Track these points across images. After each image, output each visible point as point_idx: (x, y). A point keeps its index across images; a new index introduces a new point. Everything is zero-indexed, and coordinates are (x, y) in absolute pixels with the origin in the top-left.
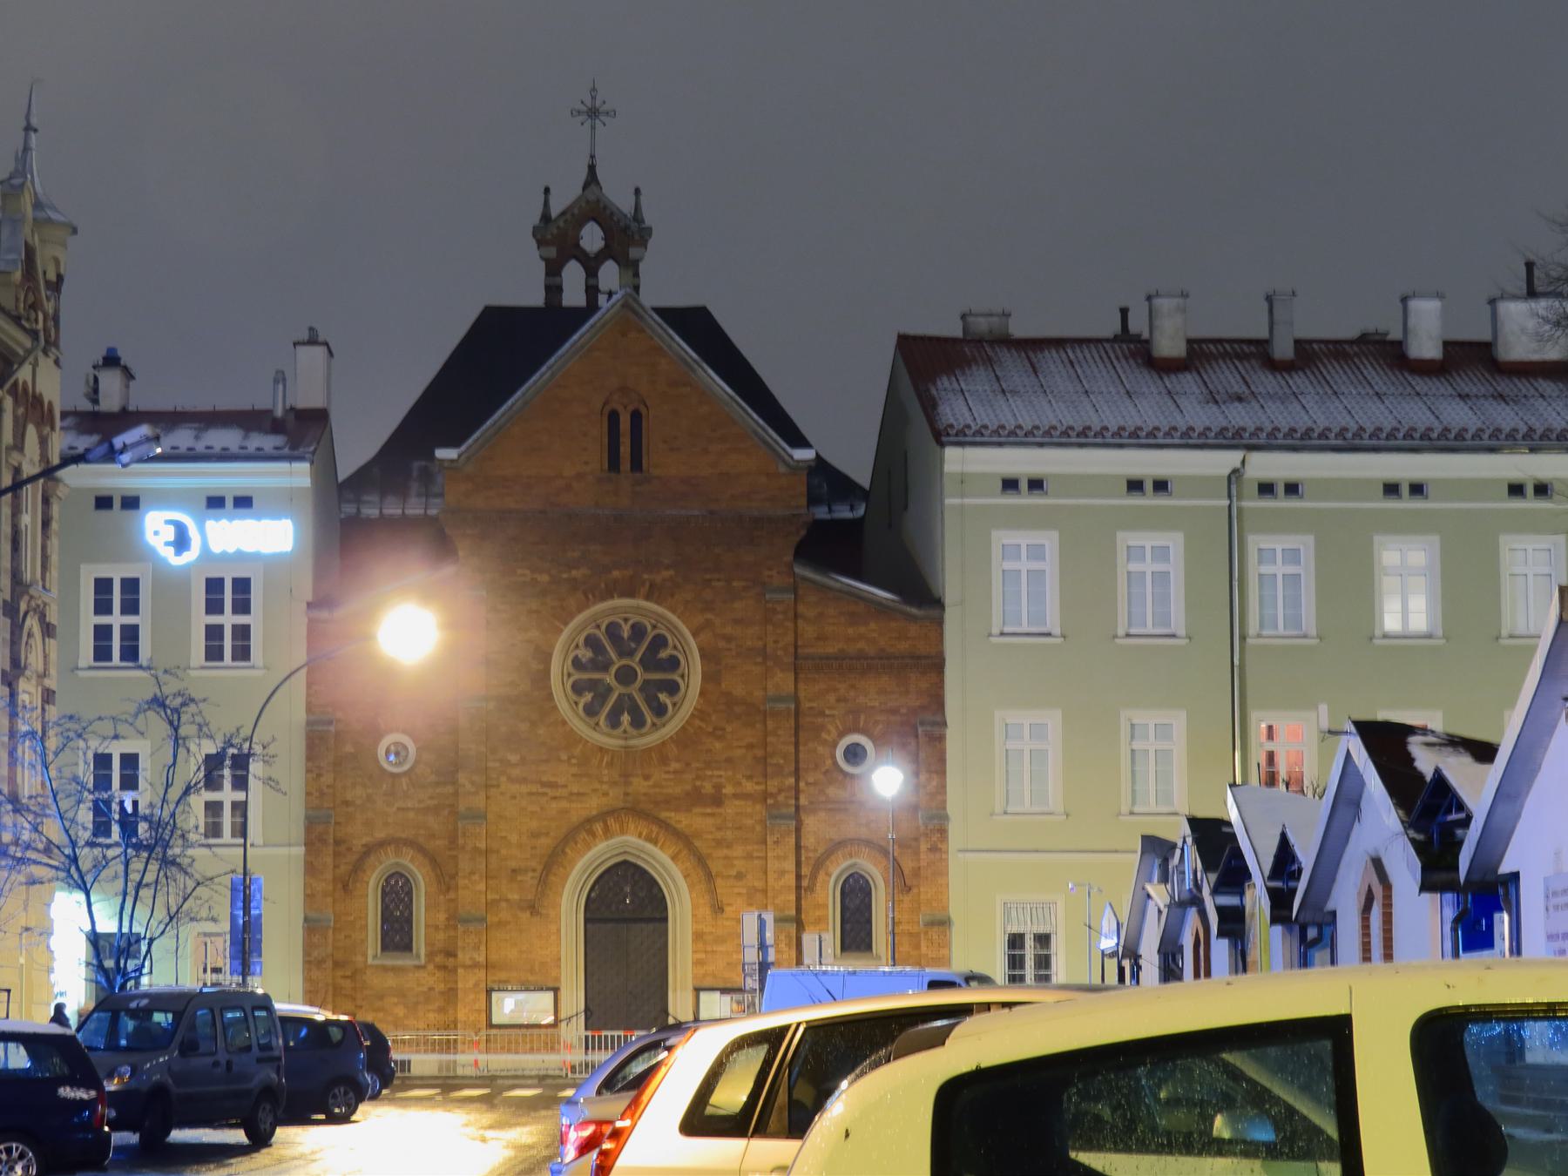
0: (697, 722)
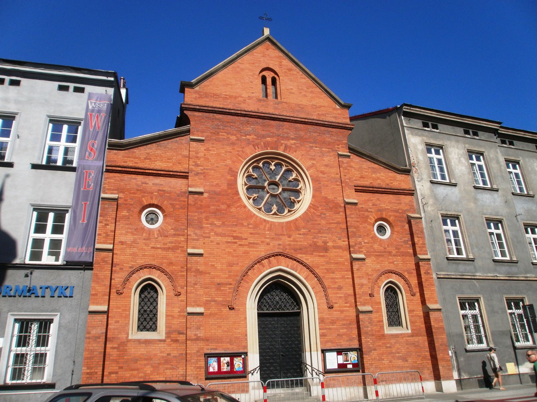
0: (312, 210)
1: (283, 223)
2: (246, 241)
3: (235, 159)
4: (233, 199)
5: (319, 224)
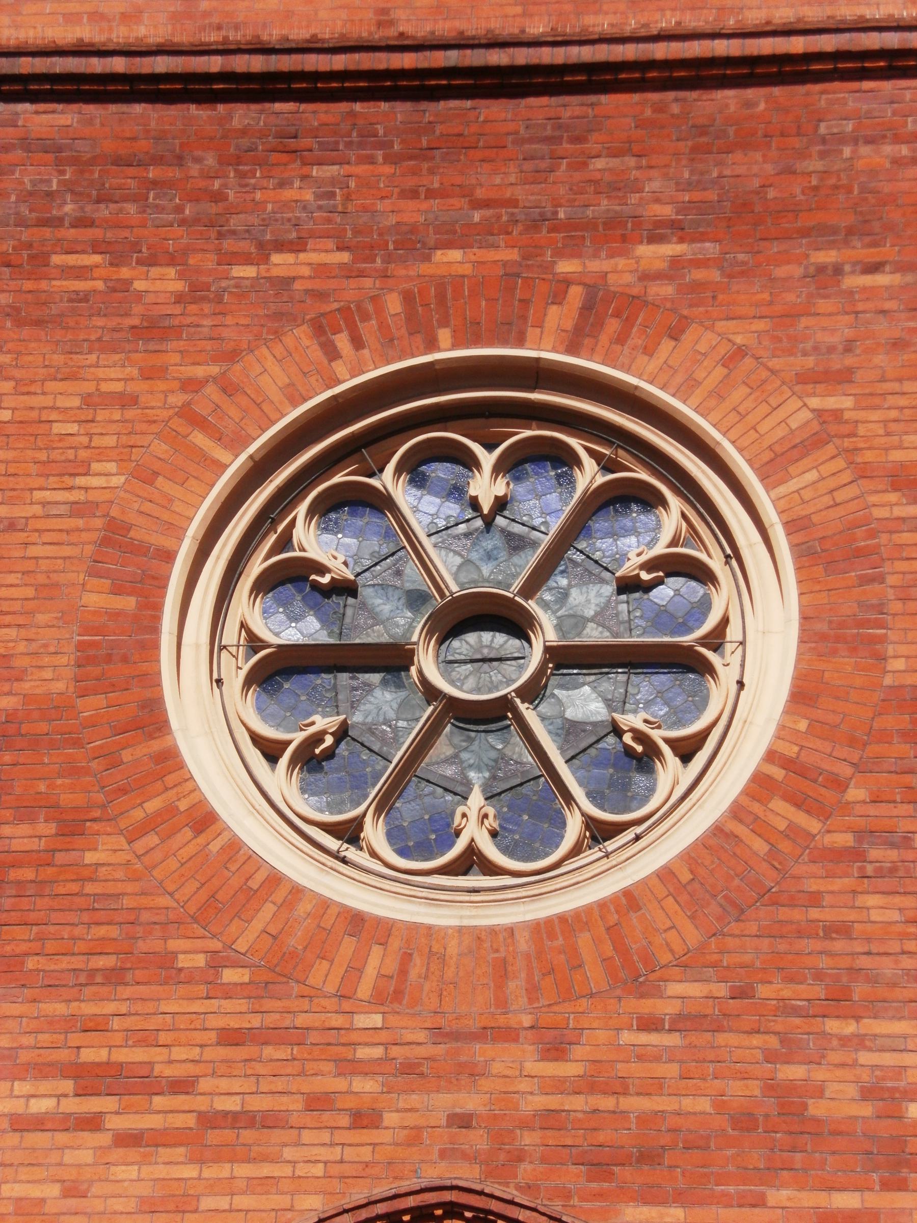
0: (782, 812)
1: (510, 931)
2: (180, 1101)
3: (160, 448)
4: (115, 764)
5: (843, 930)
